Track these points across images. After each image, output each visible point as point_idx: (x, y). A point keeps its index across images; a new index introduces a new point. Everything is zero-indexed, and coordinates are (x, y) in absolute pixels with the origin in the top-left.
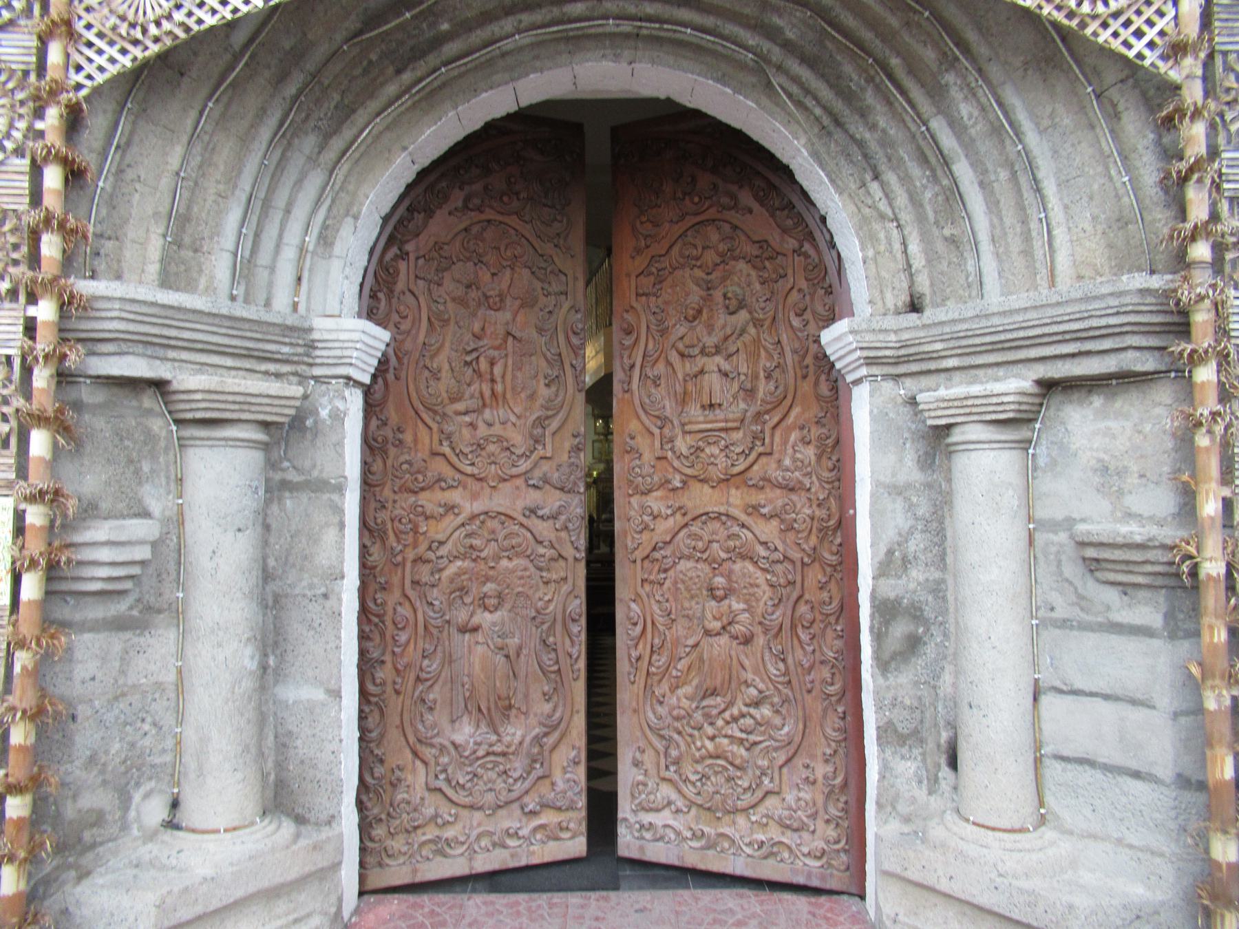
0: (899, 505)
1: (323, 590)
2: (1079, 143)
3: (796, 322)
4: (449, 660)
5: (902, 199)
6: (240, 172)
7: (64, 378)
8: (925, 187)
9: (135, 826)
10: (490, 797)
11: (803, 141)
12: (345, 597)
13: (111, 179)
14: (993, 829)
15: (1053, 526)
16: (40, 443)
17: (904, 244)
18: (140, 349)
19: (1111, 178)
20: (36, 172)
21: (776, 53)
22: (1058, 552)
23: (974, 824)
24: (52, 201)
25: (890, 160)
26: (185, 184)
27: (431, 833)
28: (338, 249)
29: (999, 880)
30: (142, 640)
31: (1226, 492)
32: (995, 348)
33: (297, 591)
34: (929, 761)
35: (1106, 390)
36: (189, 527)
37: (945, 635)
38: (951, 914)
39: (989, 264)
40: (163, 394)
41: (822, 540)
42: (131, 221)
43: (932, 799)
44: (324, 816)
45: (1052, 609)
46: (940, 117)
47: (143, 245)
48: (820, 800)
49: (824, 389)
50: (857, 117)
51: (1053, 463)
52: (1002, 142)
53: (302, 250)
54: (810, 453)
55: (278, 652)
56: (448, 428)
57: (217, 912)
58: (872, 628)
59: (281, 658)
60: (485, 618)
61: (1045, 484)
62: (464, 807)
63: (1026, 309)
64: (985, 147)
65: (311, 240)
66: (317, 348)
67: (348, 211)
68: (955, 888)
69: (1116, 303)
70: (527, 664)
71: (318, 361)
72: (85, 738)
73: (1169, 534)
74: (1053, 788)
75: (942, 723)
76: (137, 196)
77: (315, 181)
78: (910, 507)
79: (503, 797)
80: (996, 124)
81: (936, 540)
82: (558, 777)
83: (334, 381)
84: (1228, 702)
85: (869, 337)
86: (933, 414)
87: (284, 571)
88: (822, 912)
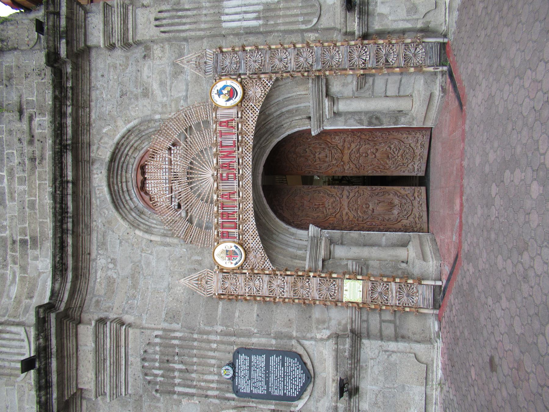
0: (349, 121)
3: (309, 140)
4: (379, 215)
5: (288, 120)
6: (281, 248)
7: (322, 272)
10: (410, 207)
15: (354, 93)
16: (334, 275)
18: (317, 262)
20: (288, 275)
21: (258, 145)
24: (293, 273)
27: (417, 219)
28: (295, 232)
31: (348, 69)
36: (350, 258)
41: (355, 135)
44: (409, 237)
47: (297, 263)
48: (411, 136)
54: (337, 137)
56: (330, 214)
60: (371, 207)
61: (346, 95)
70: (381, 199)
72: (388, 273)
73: (355, 79)
77: (281, 236)
78: (349, 119)
82: (407, 193)
84: (385, 70)
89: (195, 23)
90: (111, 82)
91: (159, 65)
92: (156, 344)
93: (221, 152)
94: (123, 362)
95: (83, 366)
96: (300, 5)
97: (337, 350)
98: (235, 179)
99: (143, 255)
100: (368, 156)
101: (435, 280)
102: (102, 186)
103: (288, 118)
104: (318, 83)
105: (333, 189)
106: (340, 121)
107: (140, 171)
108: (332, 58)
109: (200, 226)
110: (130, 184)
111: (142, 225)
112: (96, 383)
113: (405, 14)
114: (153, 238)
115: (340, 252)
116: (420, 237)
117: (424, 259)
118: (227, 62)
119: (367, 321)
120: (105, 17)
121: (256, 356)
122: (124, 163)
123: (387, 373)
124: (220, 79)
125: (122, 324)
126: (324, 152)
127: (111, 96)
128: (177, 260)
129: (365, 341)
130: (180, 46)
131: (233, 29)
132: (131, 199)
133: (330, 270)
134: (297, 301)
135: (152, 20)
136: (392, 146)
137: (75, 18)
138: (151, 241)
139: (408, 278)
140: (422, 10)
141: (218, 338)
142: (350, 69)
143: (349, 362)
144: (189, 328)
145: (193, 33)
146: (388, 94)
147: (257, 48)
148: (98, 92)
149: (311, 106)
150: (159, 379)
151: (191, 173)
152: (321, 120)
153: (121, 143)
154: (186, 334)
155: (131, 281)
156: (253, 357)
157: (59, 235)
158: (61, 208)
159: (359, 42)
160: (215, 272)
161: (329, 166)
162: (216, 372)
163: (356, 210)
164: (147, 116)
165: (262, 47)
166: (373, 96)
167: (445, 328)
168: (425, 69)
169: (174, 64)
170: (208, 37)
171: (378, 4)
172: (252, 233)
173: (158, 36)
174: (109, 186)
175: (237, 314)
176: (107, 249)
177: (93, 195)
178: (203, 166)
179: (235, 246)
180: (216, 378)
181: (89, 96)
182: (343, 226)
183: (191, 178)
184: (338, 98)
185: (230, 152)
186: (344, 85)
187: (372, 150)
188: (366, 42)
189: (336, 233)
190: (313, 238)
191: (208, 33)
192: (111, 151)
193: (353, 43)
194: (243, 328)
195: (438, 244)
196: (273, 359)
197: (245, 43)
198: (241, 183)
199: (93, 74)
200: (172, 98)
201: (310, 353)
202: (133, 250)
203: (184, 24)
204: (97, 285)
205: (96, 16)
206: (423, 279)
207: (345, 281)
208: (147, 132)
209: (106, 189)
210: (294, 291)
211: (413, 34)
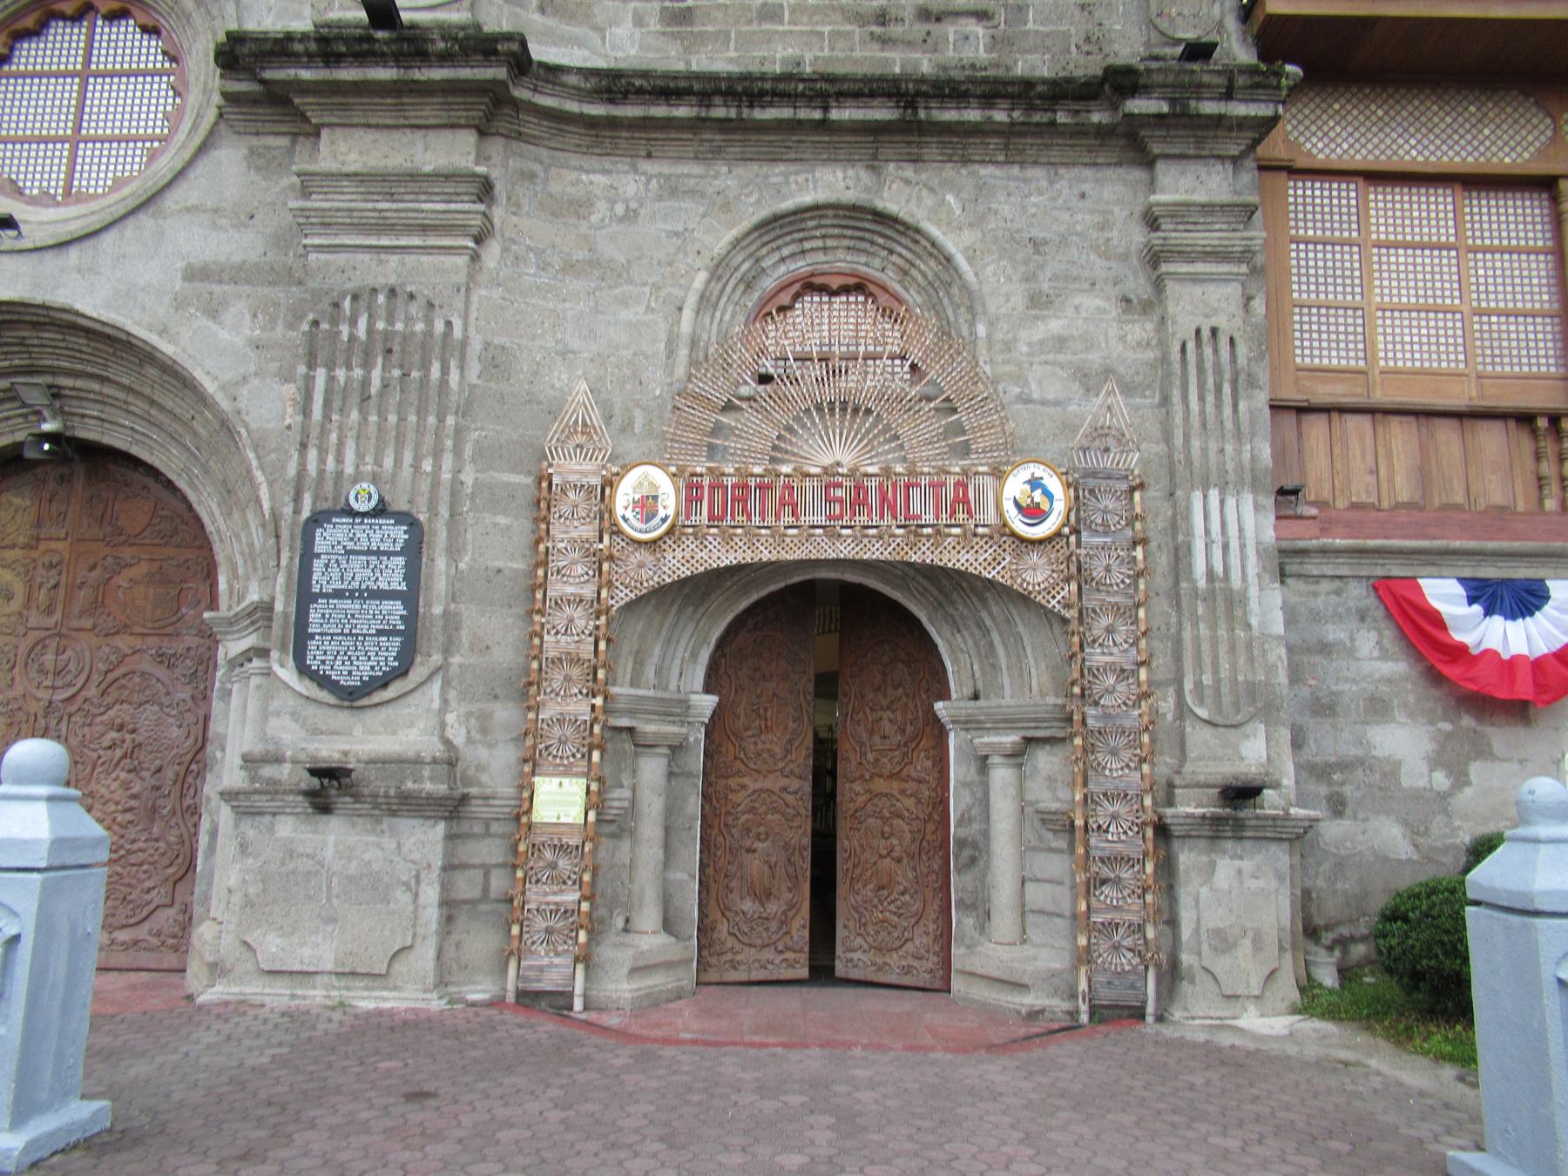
0: (967, 792)
4: (741, 866)
5: (970, 643)
7: (605, 726)
15: (1031, 804)
16: (596, 756)
24: (602, 657)
27: (729, 956)
32: (1005, 721)
36: (638, 793)
39: (1006, 680)
49: (936, 732)
54: (929, 763)
60: (759, 845)
61: (1029, 784)
72: (601, 884)
77: (691, 626)
78: (973, 793)
89: (1204, 425)
90: (1066, 216)
91: (1106, 334)
92: (429, 322)
93: (894, 485)
94: (385, 242)
95: (375, 141)
96: (1240, 678)
97: (418, 761)
98: (830, 518)
99: (647, 290)
101: (585, 996)
102: (815, 189)
103: (977, 646)
104: (1056, 719)
107: (851, 281)
108: (1114, 753)
109: (717, 430)
110: (820, 257)
111: (720, 286)
112: (333, 175)
113: (1211, 925)
114: (688, 314)
115: (652, 769)
116: (689, 961)
117: (635, 971)
118: (1109, 503)
119: (487, 834)
120: (1222, 206)
121: (405, 566)
122: (872, 243)
123: (365, 881)
124: (1069, 485)
125: (478, 240)
127: (1034, 216)
128: (634, 373)
129: (441, 828)
130: (1149, 386)
131: (1187, 517)
132: (783, 259)
133: (609, 746)
134: (535, 665)
135: (1214, 322)
136: (907, 897)
137: (1220, 133)
138: (680, 309)
139: (591, 932)
140: (1220, 965)
141: (446, 476)
142: (1085, 796)
143: (392, 792)
144: (469, 403)
145: (1178, 419)
146: (1029, 887)
147: (1139, 574)
148: (1044, 184)
149: (1003, 702)
150: (345, 330)
151: (844, 410)
152: (969, 724)
153: (918, 237)
154: (454, 398)
155: (580, 258)
156: (401, 561)
157: (696, 87)
158: (762, 93)
159: (1149, 816)
160: (604, 467)
161: (862, 744)
162: (362, 468)
163: (752, 810)
164: (984, 305)
165: (1142, 587)
166: (1025, 849)
167: (477, 1014)
168: (1083, 970)
169: (1107, 372)
170: (1170, 456)
171: (1237, 862)
172: (698, 557)
173: (1174, 334)
174: (816, 207)
175: (502, 520)
176: (660, 198)
177: (792, 168)
178: (860, 441)
179: (667, 517)
180: (349, 469)
181: (1036, 163)
182: (713, 778)
183: (832, 410)
184: (1020, 765)
185: (892, 508)
186: (1051, 780)
187: (898, 848)
188: (1150, 832)
189: (697, 761)
190: (685, 704)
191: (1179, 456)
192: (901, 214)
193: (1148, 802)
194: (469, 536)
195: (671, 1005)
196: (396, 609)
197: (1153, 545)
198: (819, 531)
199: (1088, 172)
200: (1026, 366)
201: (410, 699)
202: (659, 264)
203: (1202, 398)
204: (573, 175)
205: (1225, 185)
206: (587, 968)
207: (583, 782)
208: (946, 301)
209: (808, 199)
210: (560, 659)
211: (1166, 944)
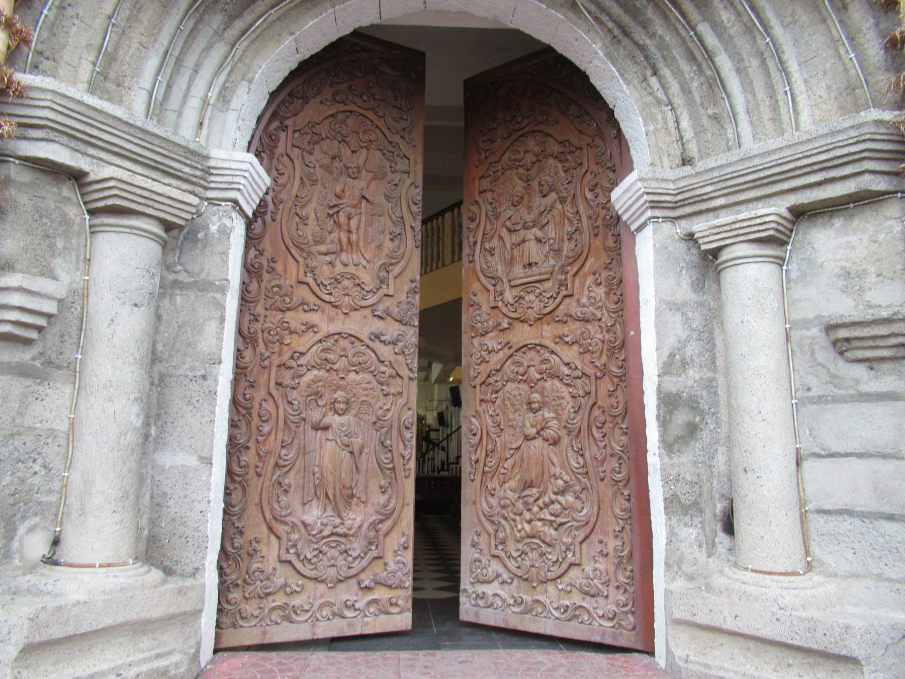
0: (678, 317)
1: (203, 372)
2: (814, 34)
3: (589, 196)
4: (303, 451)
5: (674, 88)
6: (160, 30)
8: (693, 79)
9: (17, 556)
10: (332, 572)
11: (599, 45)
12: (221, 379)
13: (54, 10)
14: (770, 573)
15: (806, 324)
17: (677, 122)
18: (65, 139)
19: (840, 58)
22: (812, 343)
23: (752, 571)
25: (665, 60)
26: (114, 29)
27: (280, 600)
28: (234, 104)
29: (779, 612)
30: (41, 389)
32: (756, 184)
33: (180, 372)
34: (707, 528)
35: (844, 212)
37: (717, 423)
38: (736, 650)
40: (81, 186)
41: (610, 357)
42: (68, 47)
43: (711, 560)
44: (189, 569)
45: (809, 389)
46: (705, 23)
47: (76, 68)
48: (612, 569)
49: (610, 242)
50: (640, 29)
51: (803, 275)
52: (754, 38)
53: (205, 102)
54: (600, 292)
55: (159, 424)
56: (313, 263)
57: (84, 635)
58: (658, 417)
59: (162, 429)
62: (310, 578)
63: (781, 148)
64: (742, 43)
65: (213, 95)
66: (212, 174)
67: (244, 76)
68: (740, 626)
69: (856, 134)
70: (367, 461)
71: (212, 185)
74: (817, 539)
75: (717, 496)
76: (74, 29)
77: (219, 50)
78: (687, 321)
79: (344, 572)
80: (749, 24)
81: (707, 347)
82: (390, 558)
83: (223, 204)
85: (653, 184)
86: (706, 240)
87: (170, 356)
88: (619, 663)
100: (532, 410)
103: (686, 90)
105: (406, 288)
106: (678, 284)
126: (546, 256)
136: (570, 498)
161: (496, 280)
163: (325, 364)
182: (260, 309)
187: (553, 423)
